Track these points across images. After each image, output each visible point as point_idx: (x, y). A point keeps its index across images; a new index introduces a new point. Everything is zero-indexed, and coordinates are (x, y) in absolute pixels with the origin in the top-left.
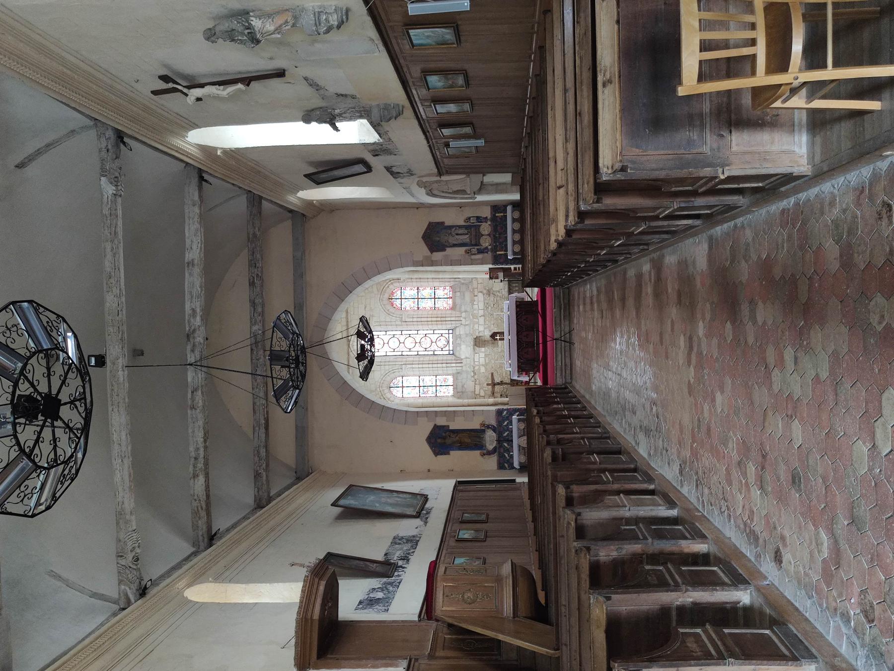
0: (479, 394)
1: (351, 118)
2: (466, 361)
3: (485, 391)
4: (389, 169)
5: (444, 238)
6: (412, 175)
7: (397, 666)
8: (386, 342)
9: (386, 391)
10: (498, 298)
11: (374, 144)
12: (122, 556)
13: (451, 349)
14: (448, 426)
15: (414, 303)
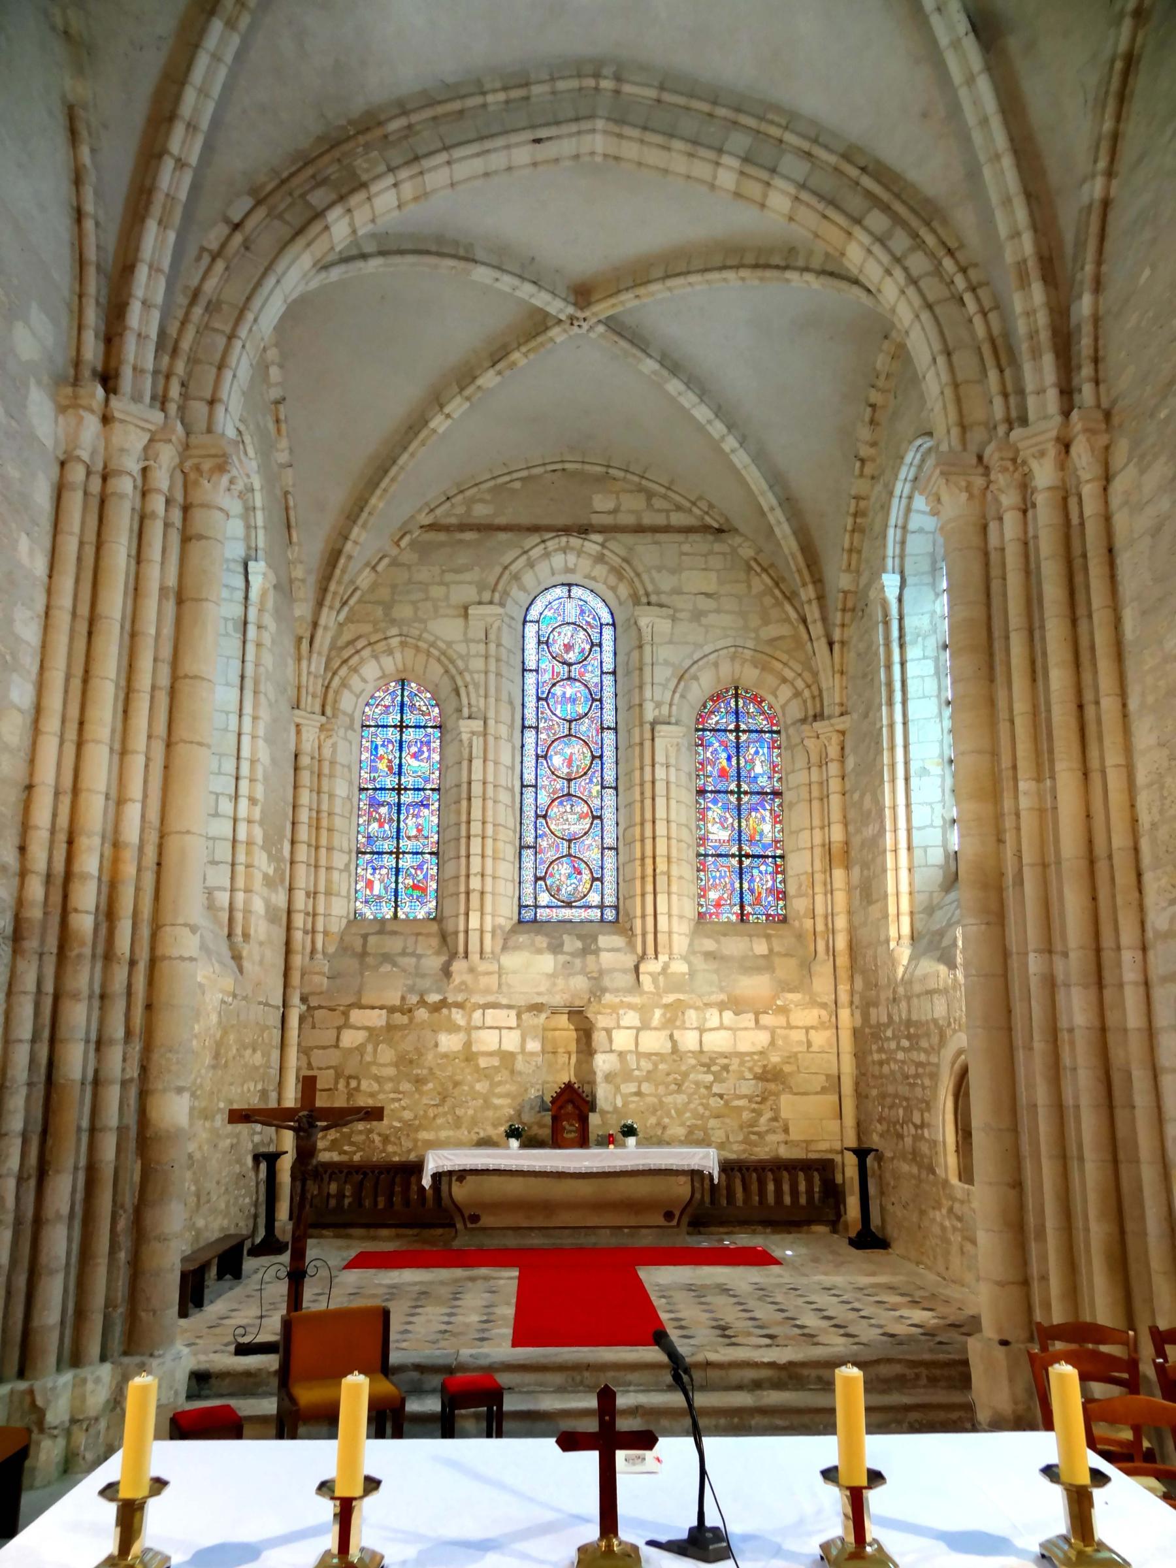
3: (360, 1049)
8: (575, 671)
9: (389, 663)
10: (746, 1116)
13: (543, 914)
15: (723, 774)
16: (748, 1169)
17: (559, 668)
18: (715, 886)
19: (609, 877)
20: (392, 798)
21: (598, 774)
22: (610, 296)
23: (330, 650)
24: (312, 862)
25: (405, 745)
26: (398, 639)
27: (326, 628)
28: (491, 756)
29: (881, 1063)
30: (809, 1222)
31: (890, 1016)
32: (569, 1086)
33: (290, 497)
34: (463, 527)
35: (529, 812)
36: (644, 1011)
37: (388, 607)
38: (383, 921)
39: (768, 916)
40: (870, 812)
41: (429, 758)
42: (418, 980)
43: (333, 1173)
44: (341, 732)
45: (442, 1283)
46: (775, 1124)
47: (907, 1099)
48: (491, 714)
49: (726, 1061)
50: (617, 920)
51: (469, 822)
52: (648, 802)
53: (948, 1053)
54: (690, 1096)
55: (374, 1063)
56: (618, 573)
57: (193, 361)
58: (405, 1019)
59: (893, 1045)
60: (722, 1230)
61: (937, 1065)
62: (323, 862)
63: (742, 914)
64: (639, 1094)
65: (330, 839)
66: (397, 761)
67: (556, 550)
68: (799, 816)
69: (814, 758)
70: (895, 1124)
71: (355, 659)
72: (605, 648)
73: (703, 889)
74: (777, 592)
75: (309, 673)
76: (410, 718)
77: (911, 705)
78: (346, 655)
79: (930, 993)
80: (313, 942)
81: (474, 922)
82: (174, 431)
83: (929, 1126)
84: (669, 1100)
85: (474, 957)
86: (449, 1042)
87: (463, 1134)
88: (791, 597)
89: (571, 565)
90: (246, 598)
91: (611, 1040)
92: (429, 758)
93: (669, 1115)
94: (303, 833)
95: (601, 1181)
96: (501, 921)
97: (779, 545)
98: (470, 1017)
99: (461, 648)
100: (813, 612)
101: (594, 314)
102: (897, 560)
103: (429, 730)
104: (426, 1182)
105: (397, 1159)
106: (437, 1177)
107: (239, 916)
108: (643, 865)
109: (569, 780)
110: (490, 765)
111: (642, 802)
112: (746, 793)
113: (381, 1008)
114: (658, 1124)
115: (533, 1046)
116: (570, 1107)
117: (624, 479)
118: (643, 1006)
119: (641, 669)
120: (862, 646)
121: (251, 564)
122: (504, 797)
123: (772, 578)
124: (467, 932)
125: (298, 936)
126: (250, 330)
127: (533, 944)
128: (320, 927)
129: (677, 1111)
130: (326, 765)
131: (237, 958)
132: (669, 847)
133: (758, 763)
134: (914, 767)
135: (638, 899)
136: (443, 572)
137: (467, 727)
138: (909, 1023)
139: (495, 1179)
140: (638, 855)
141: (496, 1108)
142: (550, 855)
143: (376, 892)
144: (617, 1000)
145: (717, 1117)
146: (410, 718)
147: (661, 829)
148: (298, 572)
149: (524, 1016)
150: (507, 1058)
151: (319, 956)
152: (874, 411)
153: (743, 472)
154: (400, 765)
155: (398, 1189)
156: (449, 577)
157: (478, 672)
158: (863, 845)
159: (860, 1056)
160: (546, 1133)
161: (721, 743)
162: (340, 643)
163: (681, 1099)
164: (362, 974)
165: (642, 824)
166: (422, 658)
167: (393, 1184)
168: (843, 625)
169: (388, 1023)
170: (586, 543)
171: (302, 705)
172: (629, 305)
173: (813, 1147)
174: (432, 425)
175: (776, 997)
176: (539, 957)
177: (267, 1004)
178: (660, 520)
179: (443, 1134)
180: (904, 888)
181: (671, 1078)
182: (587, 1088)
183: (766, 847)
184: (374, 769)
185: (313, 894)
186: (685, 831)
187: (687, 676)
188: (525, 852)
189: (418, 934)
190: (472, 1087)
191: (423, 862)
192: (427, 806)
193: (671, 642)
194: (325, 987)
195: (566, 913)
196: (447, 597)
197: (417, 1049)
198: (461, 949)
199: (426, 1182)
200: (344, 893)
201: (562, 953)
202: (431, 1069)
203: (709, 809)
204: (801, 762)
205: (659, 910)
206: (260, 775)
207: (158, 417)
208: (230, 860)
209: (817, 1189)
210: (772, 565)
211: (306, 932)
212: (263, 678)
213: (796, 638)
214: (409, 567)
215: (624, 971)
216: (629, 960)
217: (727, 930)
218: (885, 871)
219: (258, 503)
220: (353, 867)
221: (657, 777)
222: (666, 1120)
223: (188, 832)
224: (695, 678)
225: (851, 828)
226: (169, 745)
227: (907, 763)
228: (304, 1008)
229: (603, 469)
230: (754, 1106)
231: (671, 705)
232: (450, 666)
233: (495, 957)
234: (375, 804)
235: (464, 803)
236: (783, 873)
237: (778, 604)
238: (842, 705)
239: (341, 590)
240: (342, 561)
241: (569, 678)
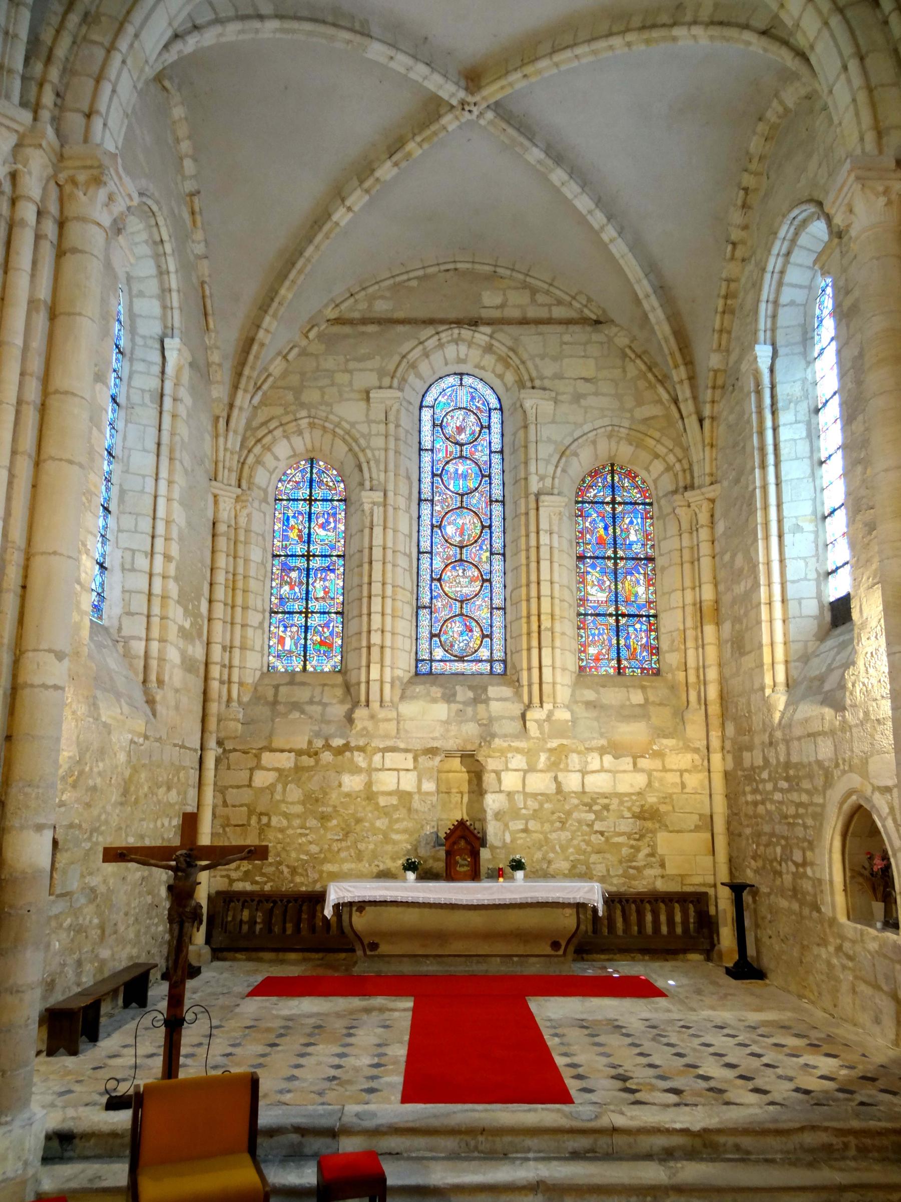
0: (259, 766)
2: (388, 720)
3: (271, 788)
9: (297, 442)
10: (625, 851)
13: (437, 667)
15: (600, 542)
16: (627, 901)
17: (451, 448)
18: (594, 643)
19: (498, 634)
20: (301, 563)
21: (487, 542)
22: (499, 78)
23: (246, 430)
24: (229, 619)
25: (313, 517)
26: (307, 420)
27: (241, 409)
28: (390, 524)
29: (755, 804)
30: (685, 951)
31: (766, 760)
32: (461, 824)
33: (206, 287)
34: (364, 321)
35: (426, 576)
37: (297, 392)
38: (293, 673)
39: (643, 669)
40: (741, 570)
41: (335, 528)
42: (323, 726)
43: (245, 901)
44: (256, 504)
45: (338, 1015)
46: (653, 859)
47: (786, 838)
48: (391, 487)
49: (606, 801)
50: (505, 673)
51: (370, 584)
52: (533, 565)
53: (836, 794)
54: (574, 832)
55: (283, 801)
56: (504, 361)
57: (68, 71)
58: (311, 762)
59: (769, 786)
60: (603, 957)
61: (823, 806)
62: (238, 619)
63: (619, 668)
64: (525, 830)
65: (244, 599)
66: (306, 531)
67: (449, 342)
68: (671, 578)
69: (685, 526)
70: (771, 862)
71: (269, 437)
72: (493, 430)
73: (583, 645)
74: (650, 375)
75: (226, 449)
76: (318, 493)
77: (784, 467)
78: (260, 434)
79: (813, 735)
80: (229, 692)
81: (375, 674)
82: (43, 135)
83: (812, 864)
84: (553, 836)
85: (375, 705)
86: (352, 783)
87: (364, 867)
88: (664, 380)
89: (462, 356)
90: (163, 372)
91: (499, 781)
92: (335, 528)
93: (553, 850)
94: (220, 593)
95: (490, 912)
96: (399, 673)
97: (653, 331)
98: (371, 760)
99: (364, 428)
100: (684, 392)
101: (484, 98)
102: (769, 333)
103: (335, 503)
104: (328, 912)
105: (304, 889)
106: (337, 907)
107: (154, 664)
108: (529, 622)
109: (461, 548)
110: (390, 533)
111: (528, 565)
112: (622, 559)
113: (290, 751)
114: (544, 859)
115: (429, 786)
116: (462, 843)
117: (511, 277)
118: (529, 751)
119: (526, 447)
120: (732, 418)
121: (167, 341)
122: (403, 562)
123: (645, 363)
124: (368, 682)
125: (215, 685)
126: (131, 46)
127: (428, 694)
128: (235, 678)
129: (561, 847)
130: (241, 533)
131: (151, 702)
132: (552, 605)
133: (632, 531)
134: (787, 525)
135: (525, 653)
136: (348, 361)
137: (369, 498)
138: (788, 765)
139: (393, 910)
140: (524, 613)
141: (395, 843)
142: (444, 614)
143: (287, 647)
144: (505, 745)
145: (599, 852)
146: (318, 493)
147: (545, 589)
148: (215, 357)
149: (421, 759)
150: (404, 797)
151: (234, 704)
152: (747, 194)
153: (622, 262)
154: (309, 535)
155: (304, 916)
156: (352, 365)
157: (379, 449)
158: (734, 602)
159: (731, 798)
160: (440, 866)
161: (599, 514)
162: (255, 424)
163: (565, 835)
164: (273, 721)
165: (528, 585)
166: (329, 436)
167: (300, 912)
168: (713, 402)
169: (296, 764)
170: (477, 335)
171: (220, 477)
172: (518, 86)
173: (688, 881)
174: (335, 217)
175: (652, 742)
176: (435, 706)
177: (183, 747)
178: (543, 313)
179: (346, 867)
180: (779, 637)
181: (555, 817)
182: (478, 825)
183: (640, 607)
184: (286, 538)
185: (228, 648)
186: (566, 592)
187: (568, 452)
188: (421, 612)
189: (324, 685)
190: (372, 824)
191: (330, 621)
192: (333, 571)
193: (553, 422)
194: (239, 733)
195: (459, 667)
196: (351, 383)
197: (322, 788)
198: (363, 698)
199: (328, 912)
200: (258, 647)
201: (455, 702)
202: (335, 807)
203: (588, 573)
204: (672, 529)
205: (544, 663)
206: (175, 534)
207: (26, 116)
208: (145, 612)
209: (692, 920)
210: (645, 352)
211: (222, 682)
212: (178, 447)
213: (668, 417)
214: (316, 356)
215: (512, 719)
216: (516, 709)
217: (604, 682)
218: (759, 622)
219: (174, 285)
220: (266, 625)
221: (542, 542)
222: (551, 855)
223: (55, 553)
224: (576, 454)
225: (721, 588)
226: (37, 464)
227: (780, 521)
228: (220, 751)
229: (492, 269)
230: (632, 842)
231: (553, 478)
232: (354, 444)
233: (394, 706)
234: (286, 569)
235: (366, 567)
236: (656, 630)
237: (651, 386)
238: (712, 475)
239: (255, 374)
240: (255, 347)
241: (461, 457)
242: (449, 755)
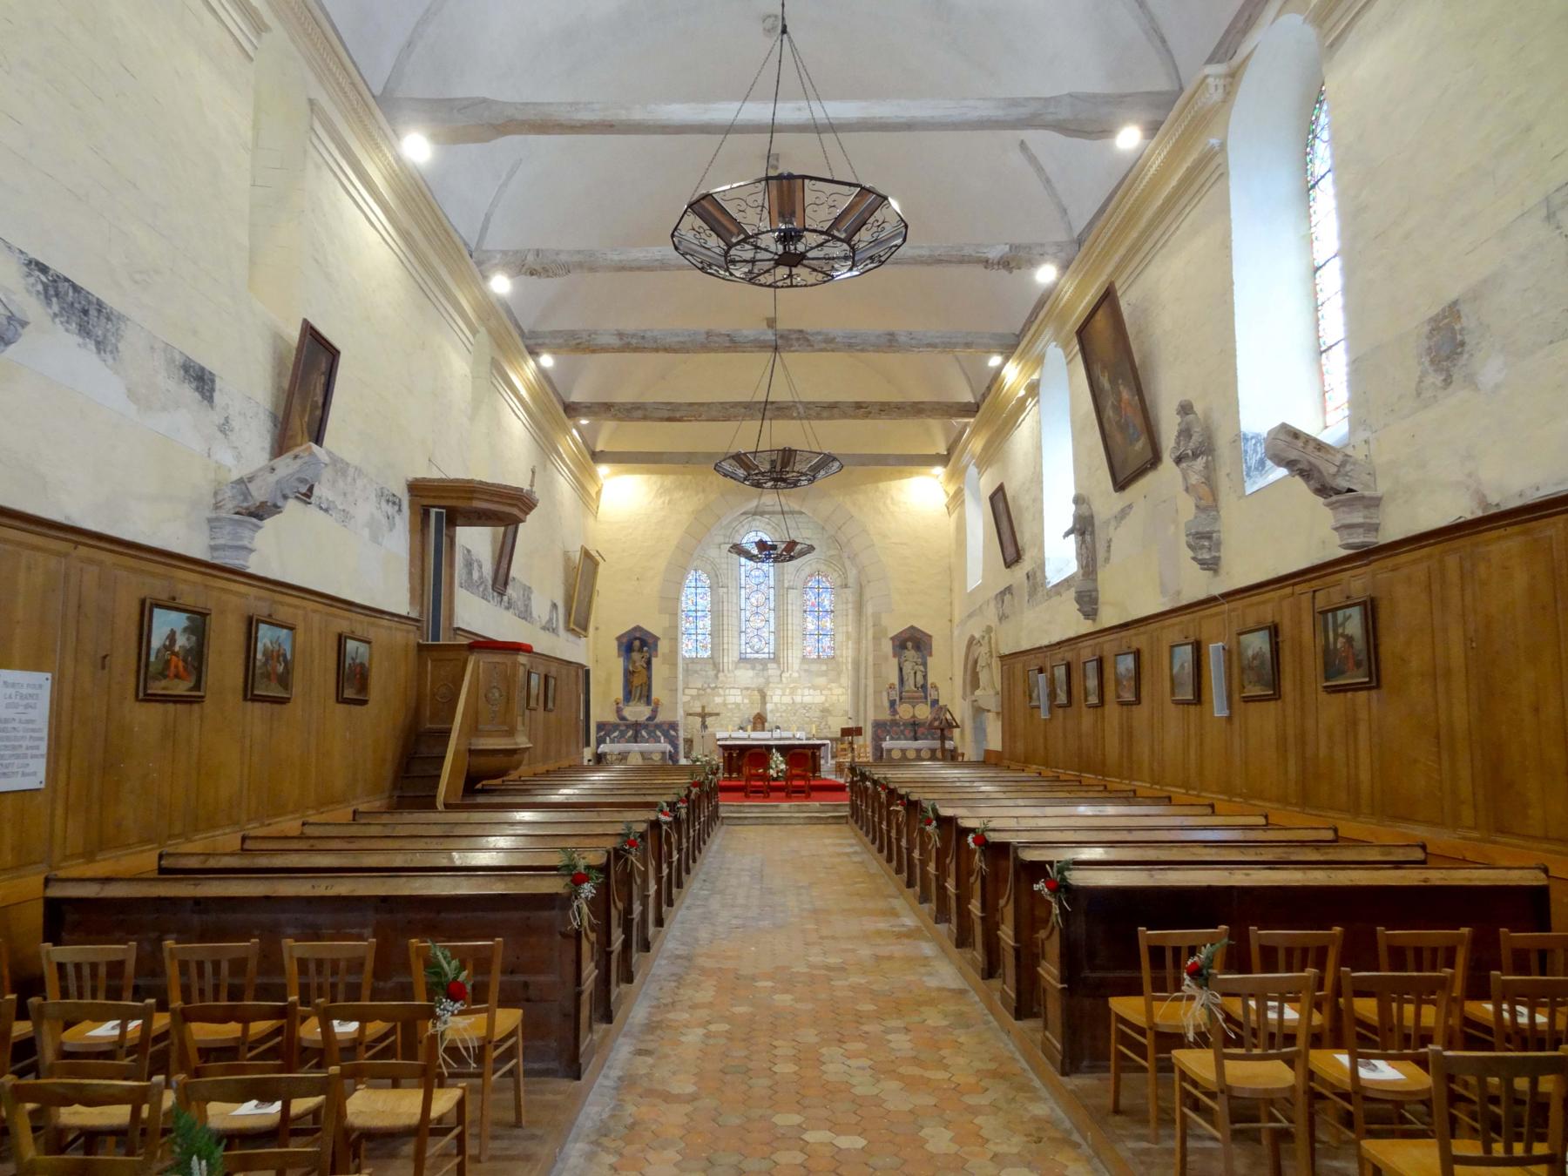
1: (1079, 556)
4: (1009, 590)
5: (911, 654)
6: (1000, 619)
7: (412, 603)
11: (1045, 578)
12: (538, 255)
13: (748, 656)
14: (656, 656)
19: (772, 642)
20: (694, 614)
32: (758, 714)
36: (783, 690)
38: (692, 658)
50: (774, 658)
76: (699, 584)
81: (725, 660)
85: (726, 671)
86: (718, 700)
115: (746, 701)
122: (735, 615)
142: (751, 635)
146: (699, 584)
147: (790, 627)
150: (738, 705)
163: (795, 718)
195: (756, 656)
216: (779, 672)
234: (688, 617)
242: (753, 690)
